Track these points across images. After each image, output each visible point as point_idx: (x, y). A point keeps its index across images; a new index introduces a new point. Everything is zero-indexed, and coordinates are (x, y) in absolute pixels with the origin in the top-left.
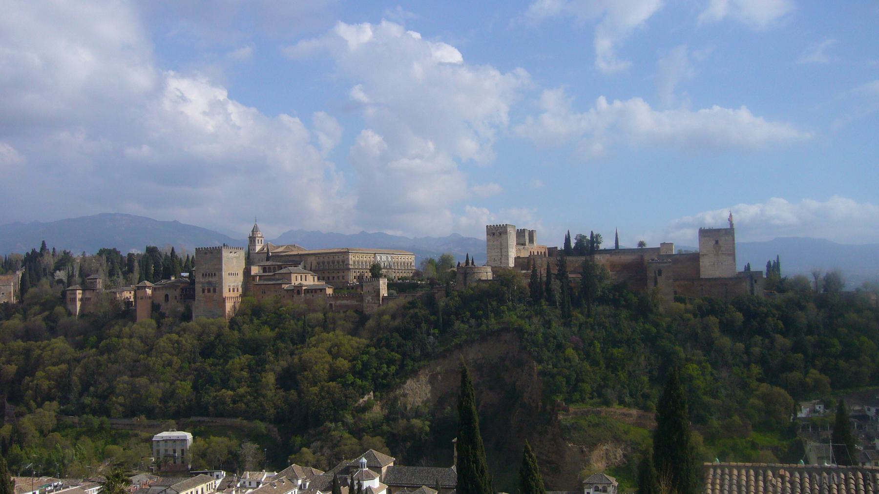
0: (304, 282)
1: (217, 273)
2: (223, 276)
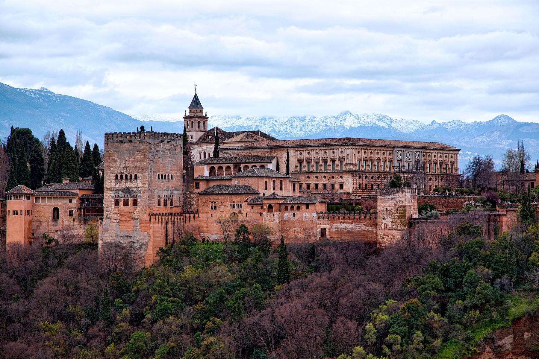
0: (278, 192)
1: (139, 174)
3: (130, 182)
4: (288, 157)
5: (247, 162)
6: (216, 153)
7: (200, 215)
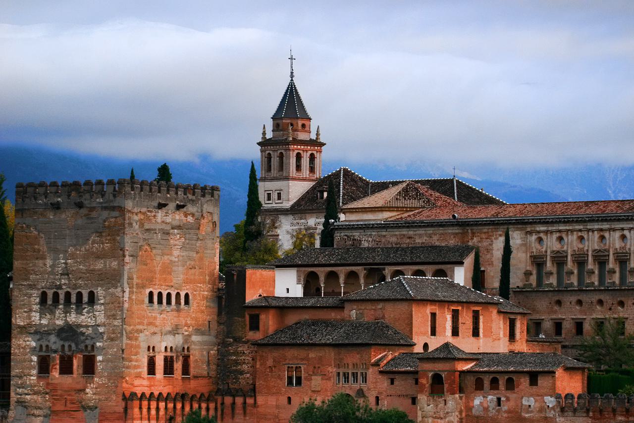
0: (466, 344)
1: (100, 292)
2: (126, 305)
3: (77, 310)
4: (507, 251)
5: (400, 260)
6: (328, 236)
7: (260, 400)
